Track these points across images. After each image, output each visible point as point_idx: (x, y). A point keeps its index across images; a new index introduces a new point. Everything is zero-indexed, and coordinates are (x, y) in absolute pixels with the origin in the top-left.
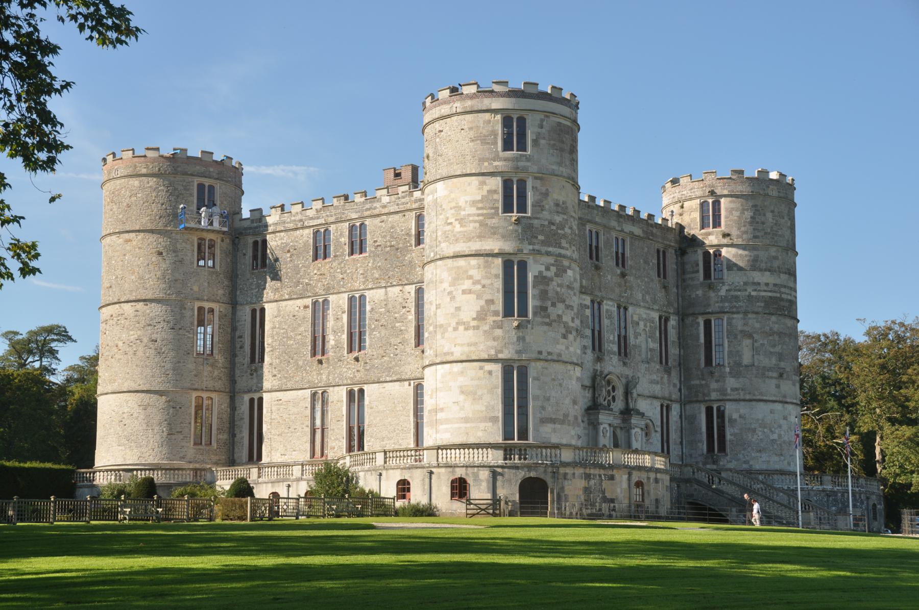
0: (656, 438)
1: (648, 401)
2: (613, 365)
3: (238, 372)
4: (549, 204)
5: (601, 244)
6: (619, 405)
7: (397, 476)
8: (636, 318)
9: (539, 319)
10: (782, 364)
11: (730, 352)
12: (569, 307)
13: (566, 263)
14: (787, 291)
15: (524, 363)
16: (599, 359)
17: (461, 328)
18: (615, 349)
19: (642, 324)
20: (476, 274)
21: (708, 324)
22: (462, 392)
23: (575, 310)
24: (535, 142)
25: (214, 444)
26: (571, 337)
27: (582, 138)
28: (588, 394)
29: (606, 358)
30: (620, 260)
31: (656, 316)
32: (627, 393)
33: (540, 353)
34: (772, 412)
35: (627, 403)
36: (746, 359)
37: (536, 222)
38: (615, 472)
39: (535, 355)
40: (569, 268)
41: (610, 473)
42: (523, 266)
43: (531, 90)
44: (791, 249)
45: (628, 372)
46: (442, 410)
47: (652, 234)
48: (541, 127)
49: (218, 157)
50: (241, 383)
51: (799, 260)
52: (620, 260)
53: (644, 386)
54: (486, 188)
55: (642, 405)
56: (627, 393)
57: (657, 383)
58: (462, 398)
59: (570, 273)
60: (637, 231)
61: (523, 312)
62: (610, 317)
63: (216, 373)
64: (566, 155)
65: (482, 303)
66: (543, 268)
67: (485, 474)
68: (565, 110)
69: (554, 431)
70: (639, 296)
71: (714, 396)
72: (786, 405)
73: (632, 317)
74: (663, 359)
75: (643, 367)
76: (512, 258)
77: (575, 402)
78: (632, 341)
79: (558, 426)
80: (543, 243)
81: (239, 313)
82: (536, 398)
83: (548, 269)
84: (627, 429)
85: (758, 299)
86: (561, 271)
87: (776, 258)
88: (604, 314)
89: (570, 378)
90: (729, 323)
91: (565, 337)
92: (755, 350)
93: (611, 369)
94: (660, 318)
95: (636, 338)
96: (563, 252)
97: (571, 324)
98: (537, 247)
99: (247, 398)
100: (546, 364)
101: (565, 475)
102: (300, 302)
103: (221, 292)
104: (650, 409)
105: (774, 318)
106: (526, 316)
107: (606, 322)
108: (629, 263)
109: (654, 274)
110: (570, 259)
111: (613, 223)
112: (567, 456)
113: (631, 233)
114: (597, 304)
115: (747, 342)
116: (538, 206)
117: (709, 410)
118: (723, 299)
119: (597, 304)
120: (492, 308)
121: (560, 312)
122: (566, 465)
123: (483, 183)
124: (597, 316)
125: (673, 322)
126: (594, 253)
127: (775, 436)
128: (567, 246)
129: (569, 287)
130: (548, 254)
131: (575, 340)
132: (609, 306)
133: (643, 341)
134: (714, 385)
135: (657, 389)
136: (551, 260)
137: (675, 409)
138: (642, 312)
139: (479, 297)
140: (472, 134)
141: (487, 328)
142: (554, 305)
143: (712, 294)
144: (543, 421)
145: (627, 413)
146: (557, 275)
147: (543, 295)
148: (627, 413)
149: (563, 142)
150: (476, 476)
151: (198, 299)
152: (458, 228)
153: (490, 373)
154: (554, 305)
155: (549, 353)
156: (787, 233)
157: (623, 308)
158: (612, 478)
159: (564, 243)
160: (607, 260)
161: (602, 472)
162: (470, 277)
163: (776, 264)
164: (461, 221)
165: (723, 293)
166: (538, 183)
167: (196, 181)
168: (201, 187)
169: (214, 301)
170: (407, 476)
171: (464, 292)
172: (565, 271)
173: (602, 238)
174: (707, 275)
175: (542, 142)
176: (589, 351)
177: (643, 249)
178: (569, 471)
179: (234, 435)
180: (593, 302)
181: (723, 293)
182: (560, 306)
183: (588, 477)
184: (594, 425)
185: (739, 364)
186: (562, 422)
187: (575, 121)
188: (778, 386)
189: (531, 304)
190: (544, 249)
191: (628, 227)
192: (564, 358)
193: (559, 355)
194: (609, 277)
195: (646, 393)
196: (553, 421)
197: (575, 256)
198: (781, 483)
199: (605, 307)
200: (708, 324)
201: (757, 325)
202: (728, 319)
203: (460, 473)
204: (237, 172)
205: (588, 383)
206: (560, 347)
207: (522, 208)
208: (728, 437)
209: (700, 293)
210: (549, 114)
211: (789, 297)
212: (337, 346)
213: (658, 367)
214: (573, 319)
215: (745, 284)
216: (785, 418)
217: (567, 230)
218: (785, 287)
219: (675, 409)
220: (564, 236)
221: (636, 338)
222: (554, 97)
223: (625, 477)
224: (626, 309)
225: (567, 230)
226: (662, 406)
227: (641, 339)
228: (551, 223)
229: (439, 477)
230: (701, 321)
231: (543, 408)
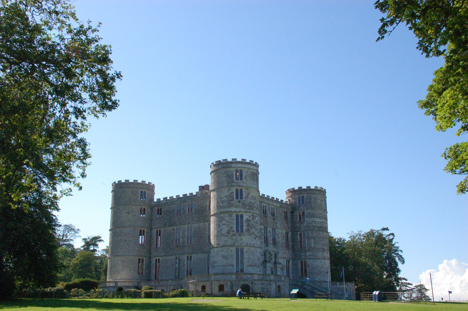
0: (285, 271)
2: (271, 248)
3: (152, 251)
4: (250, 197)
5: (267, 210)
6: (273, 260)
7: (202, 284)
8: (278, 233)
9: (247, 233)
10: (324, 247)
11: (308, 244)
12: (257, 229)
13: (255, 215)
15: (242, 247)
16: (267, 246)
17: (222, 236)
18: (272, 242)
19: (280, 234)
20: (227, 219)
21: (301, 234)
22: (222, 257)
24: (245, 177)
25: (144, 273)
26: (257, 239)
27: (260, 176)
28: (263, 257)
30: (273, 214)
31: (284, 232)
32: (276, 257)
33: (247, 244)
34: (321, 262)
35: (276, 260)
36: (313, 245)
37: (246, 202)
38: (271, 282)
39: (246, 245)
40: (256, 217)
41: (269, 282)
42: (242, 216)
43: (244, 161)
44: (326, 210)
45: (275, 249)
46: (216, 262)
48: (247, 173)
49: (147, 183)
50: (153, 254)
51: (328, 214)
52: (273, 214)
53: (280, 255)
54: (230, 192)
55: (281, 261)
56: (276, 257)
58: (222, 259)
59: (257, 218)
60: (278, 205)
61: (242, 231)
62: (270, 232)
63: (145, 250)
64: (255, 182)
65: (229, 228)
66: (248, 217)
67: (229, 284)
68: (255, 168)
69: (252, 269)
71: (303, 257)
74: (287, 246)
75: (281, 248)
76: (238, 213)
77: (258, 260)
78: (277, 240)
79: (253, 268)
80: (248, 209)
81: (153, 232)
82: (246, 258)
83: (250, 217)
84: (276, 268)
85: (316, 227)
86: (254, 218)
87: (321, 214)
88: (268, 232)
89: (257, 252)
90: (307, 234)
91: (255, 239)
92: (315, 243)
98: (246, 210)
99: (154, 259)
100: (249, 247)
101: (255, 283)
102: (172, 228)
103: (147, 225)
104: (283, 261)
105: (321, 233)
106: (243, 232)
107: (269, 234)
108: (276, 215)
109: (283, 218)
110: (257, 214)
111: (270, 203)
112: (256, 277)
113: (276, 206)
114: (266, 228)
115: (313, 240)
116: (247, 197)
117: (302, 262)
118: (305, 227)
119: (266, 228)
120: (232, 229)
122: (255, 280)
123: (229, 190)
124: (266, 232)
125: (290, 234)
126: (265, 212)
127: (322, 270)
129: (257, 223)
130: (250, 212)
132: (269, 229)
133: (281, 240)
134: (303, 254)
135: (285, 255)
136: (251, 214)
137: (291, 261)
138: (280, 231)
139: (228, 226)
140: (225, 175)
141: (230, 236)
142: (251, 228)
143: (302, 225)
144: (248, 266)
145: (275, 263)
146: (252, 219)
147: (248, 225)
148: (275, 263)
150: (227, 284)
151: (140, 227)
152: (221, 204)
153: (231, 250)
154: (251, 228)
155: (250, 244)
156: (324, 206)
157: (274, 230)
158: (270, 284)
159: (255, 209)
160: (269, 215)
161: (266, 282)
162: (225, 220)
163: (321, 216)
164: (222, 202)
165: (305, 225)
166: (246, 190)
167: (140, 190)
168: (142, 192)
169: (145, 228)
170: (204, 284)
171: (223, 224)
173: (267, 207)
174: (300, 219)
175: (248, 177)
176: (263, 243)
178: (256, 282)
179: (150, 271)
181: (305, 225)
182: (254, 229)
183: (263, 284)
184: (265, 267)
185: (311, 247)
186: (254, 266)
187: (258, 171)
188: (323, 254)
189: (245, 228)
190: (248, 211)
191: (275, 204)
192: (255, 246)
193: (254, 244)
196: (251, 266)
197: (258, 213)
198: (324, 285)
199: (268, 229)
200: (301, 234)
201: (316, 235)
202: (307, 233)
203: (222, 283)
204: (153, 187)
205: (263, 254)
206: (254, 242)
207: (242, 198)
208: (308, 271)
209: (298, 225)
210: (249, 169)
212: (184, 242)
215: (312, 222)
216: (325, 264)
217: (256, 205)
219: (291, 261)
220: (255, 207)
221: (278, 238)
222: (251, 163)
223: (274, 284)
224: (275, 230)
225: (256, 205)
227: (280, 239)
228: (250, 202)
229: (215, 284)
230: (299, 233)
231: (248, 262)
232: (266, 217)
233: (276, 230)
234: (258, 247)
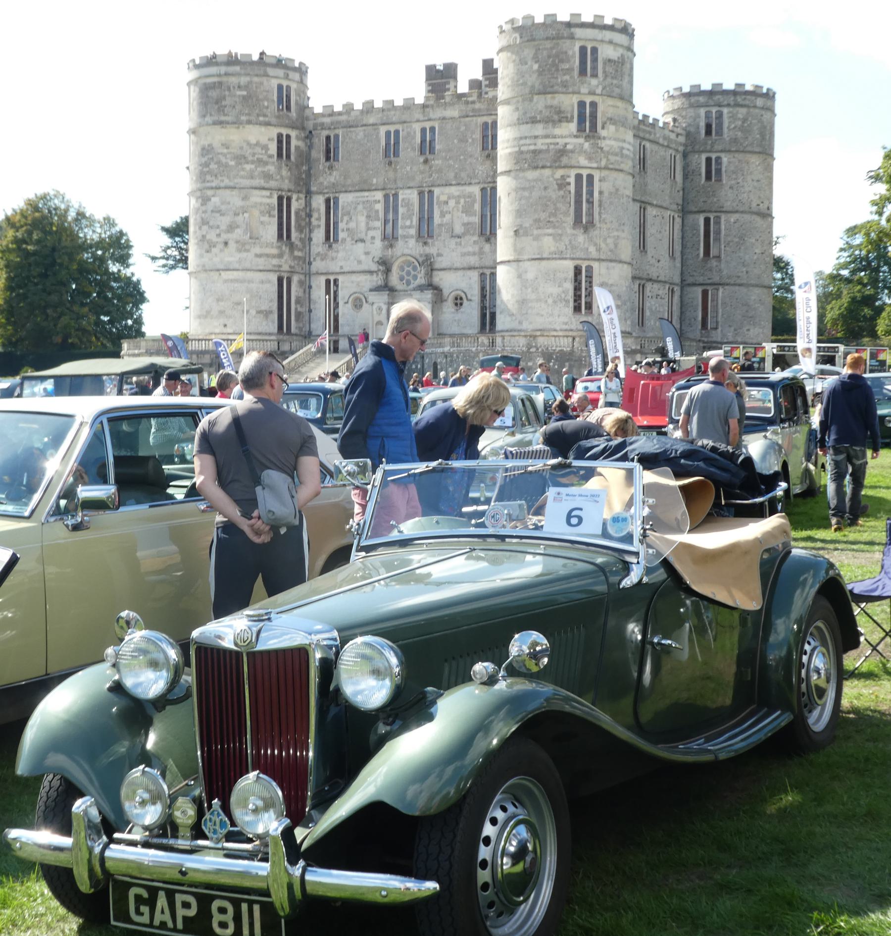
1: (460, 273)
8: (444, 198)
14: (528, 141)
18: (413, 232)
19: (452, 203)
23: (223, 227)
26: (214, 250)
29: (400, 243)
40: (213, 196)
45: (428, 250)
47: (473, 110)
57: (474, 254)
59: (213, 199)
70: (451, 175)
72: (521, 264)
73: (438, 197)
75: (454, 241)
78: (437, 220)
93: (406, 251)
94: (483, 190)
95: (443, 215)
96: (208, 185)
97: (215, 239)
107: (401, 210)
121: (204, 233)
128: (214, 178)
131: (221, 251)
135: (473, 260)
138: (454, 190)
149: (207, 97)
160: (408, 152)
172: (210, 200)
177: (458, 128)
180: (386, 197)
194: (408, 168)
195: (458, 265)
199: (400, 197)
211: (532, 148)
213: (476, 238)
214: (219, 235)
218: (526, 138)
221: (443, 215)
226: (482, 275)
232: (390, 163)
233: (437, 191)
234: (218, 270)
